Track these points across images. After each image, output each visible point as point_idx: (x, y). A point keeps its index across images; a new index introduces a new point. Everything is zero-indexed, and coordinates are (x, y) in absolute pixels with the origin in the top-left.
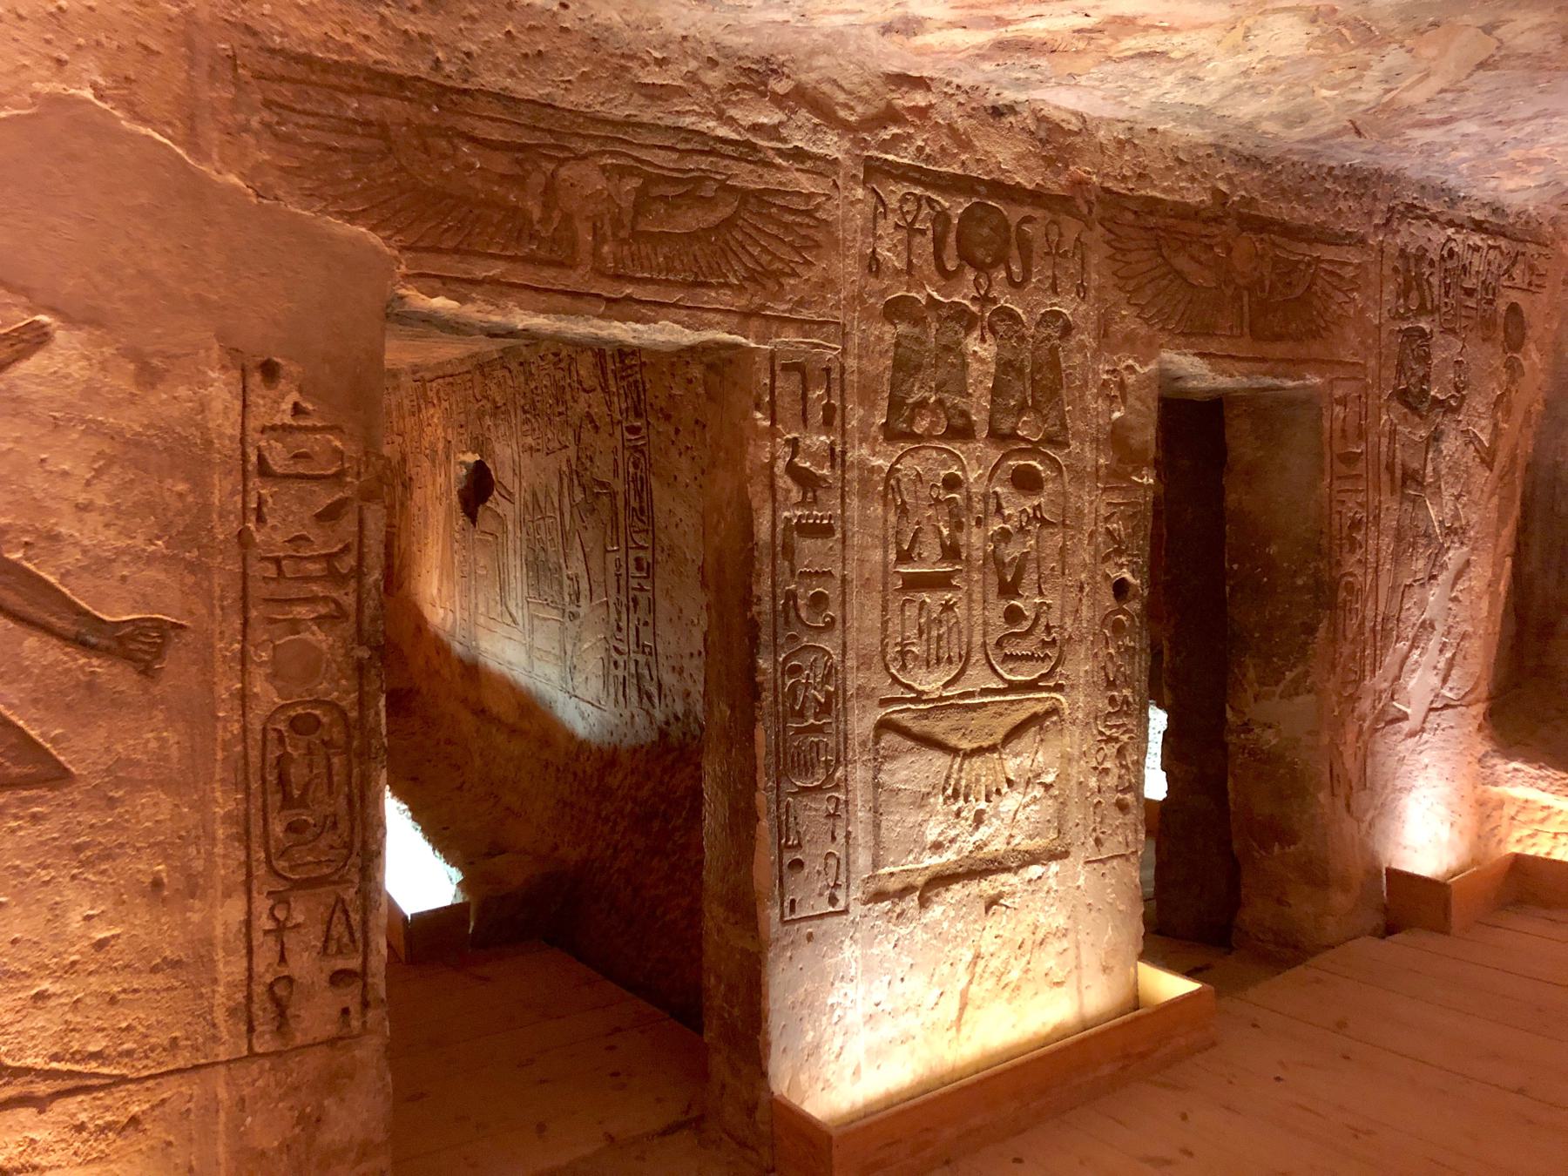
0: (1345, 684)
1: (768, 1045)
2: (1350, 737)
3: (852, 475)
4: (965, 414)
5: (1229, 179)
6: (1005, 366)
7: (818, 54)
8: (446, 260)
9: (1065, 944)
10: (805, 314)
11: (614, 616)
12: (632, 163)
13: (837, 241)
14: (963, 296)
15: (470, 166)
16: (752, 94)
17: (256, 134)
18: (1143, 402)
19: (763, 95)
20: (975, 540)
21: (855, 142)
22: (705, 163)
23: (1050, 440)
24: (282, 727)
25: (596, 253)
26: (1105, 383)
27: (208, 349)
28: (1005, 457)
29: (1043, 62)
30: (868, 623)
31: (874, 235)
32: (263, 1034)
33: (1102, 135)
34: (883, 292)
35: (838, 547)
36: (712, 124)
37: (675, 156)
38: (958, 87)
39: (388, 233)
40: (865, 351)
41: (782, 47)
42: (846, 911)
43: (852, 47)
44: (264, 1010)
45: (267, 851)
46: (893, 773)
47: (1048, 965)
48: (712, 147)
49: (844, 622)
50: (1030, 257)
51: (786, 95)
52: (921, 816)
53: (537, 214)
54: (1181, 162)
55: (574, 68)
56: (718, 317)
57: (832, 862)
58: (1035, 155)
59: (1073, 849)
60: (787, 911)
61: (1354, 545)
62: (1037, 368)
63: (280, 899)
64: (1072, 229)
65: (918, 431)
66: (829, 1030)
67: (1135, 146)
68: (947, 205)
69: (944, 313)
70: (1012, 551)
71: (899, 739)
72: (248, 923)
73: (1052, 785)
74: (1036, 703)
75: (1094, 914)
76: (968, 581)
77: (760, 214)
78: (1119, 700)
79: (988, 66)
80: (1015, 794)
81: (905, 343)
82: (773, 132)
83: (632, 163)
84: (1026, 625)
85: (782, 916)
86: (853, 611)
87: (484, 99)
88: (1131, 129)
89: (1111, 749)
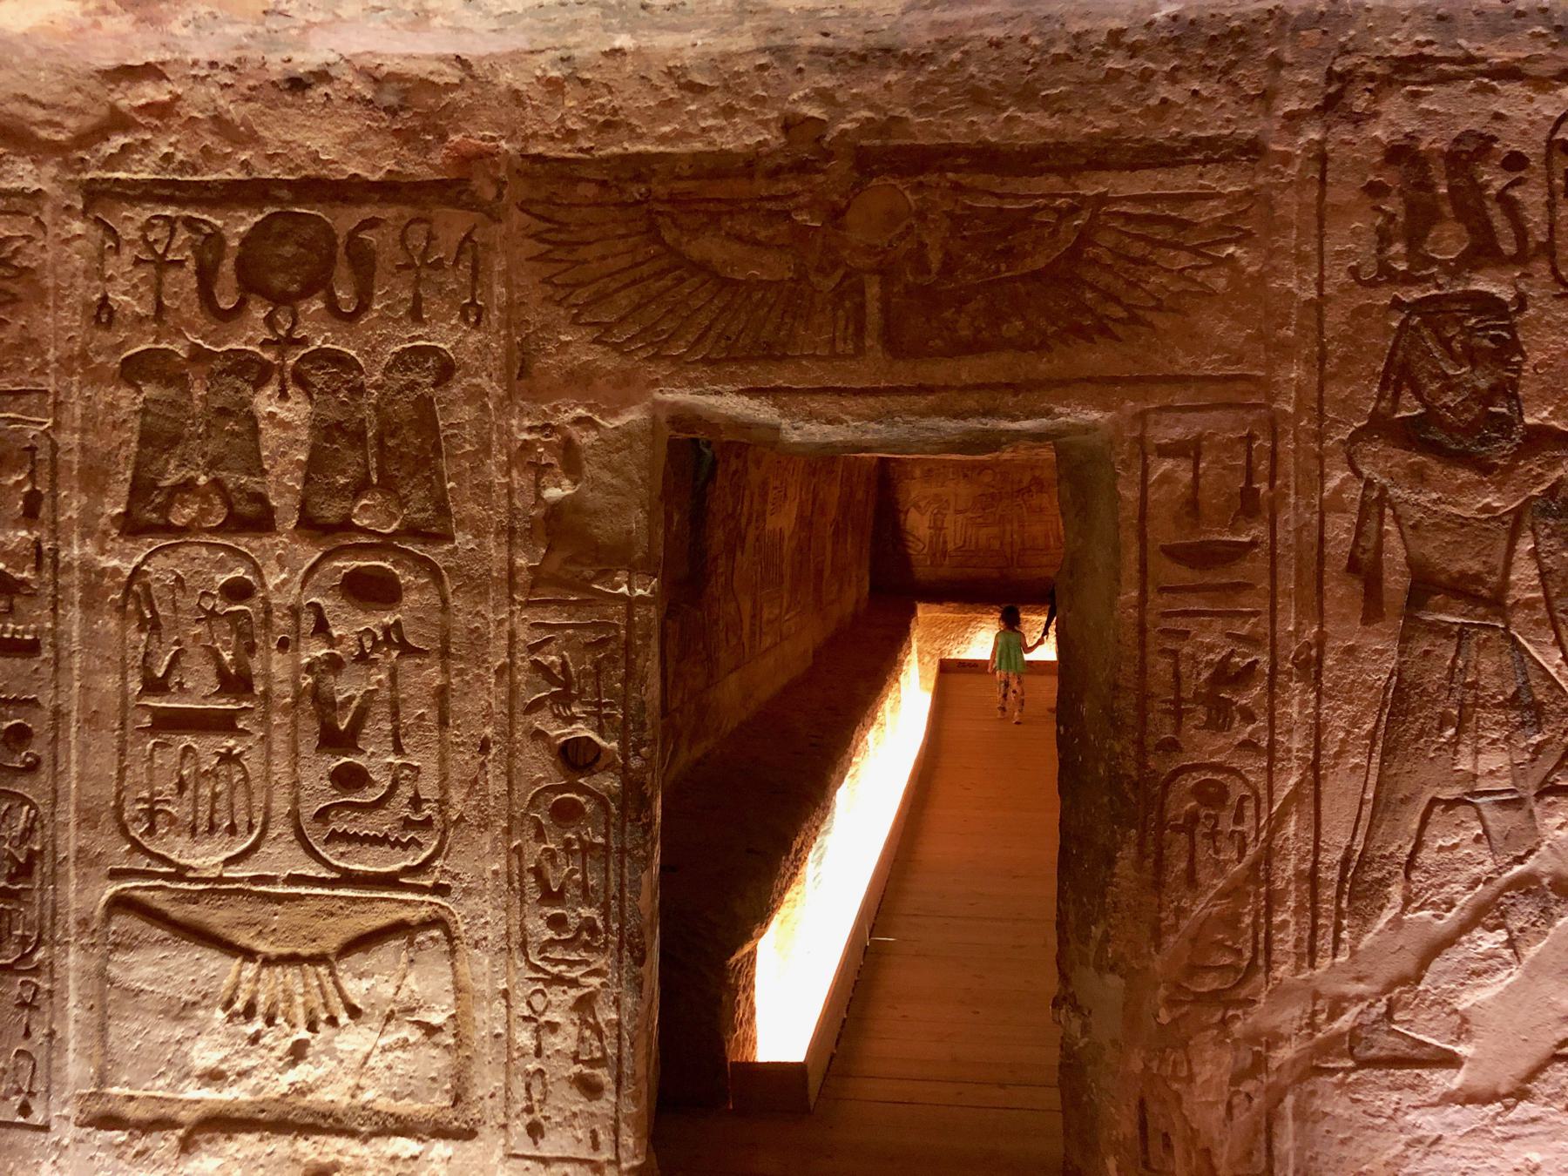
4: (261, 499)
5: (823, 96)
13: (43, 292)
14: (250, 336)
18: (616, 471)
20: (277, 670)
21: (67, 165)
23: (412, 531)
28: (327, 556)
30: (93, 769)
33: (507, 77)
34: (119, 348)
35: (48, 671)
38: (213, 64)
40: (89, 424)
42: (45, 1128)
46: (129, 968)
49: (55, 764)
50: (371, 275)
52: (179, 1032)
57: (22, 1062)
59: (484, 1131)
62: (388, 428)
65: (177, 521)
67: (585, 82)
68: (219, 223)
69: (217, 365)
74: (412, 906)
78: (573, 922)
80: (363, 1029)
81: (154, 409)
84: (371, 795)
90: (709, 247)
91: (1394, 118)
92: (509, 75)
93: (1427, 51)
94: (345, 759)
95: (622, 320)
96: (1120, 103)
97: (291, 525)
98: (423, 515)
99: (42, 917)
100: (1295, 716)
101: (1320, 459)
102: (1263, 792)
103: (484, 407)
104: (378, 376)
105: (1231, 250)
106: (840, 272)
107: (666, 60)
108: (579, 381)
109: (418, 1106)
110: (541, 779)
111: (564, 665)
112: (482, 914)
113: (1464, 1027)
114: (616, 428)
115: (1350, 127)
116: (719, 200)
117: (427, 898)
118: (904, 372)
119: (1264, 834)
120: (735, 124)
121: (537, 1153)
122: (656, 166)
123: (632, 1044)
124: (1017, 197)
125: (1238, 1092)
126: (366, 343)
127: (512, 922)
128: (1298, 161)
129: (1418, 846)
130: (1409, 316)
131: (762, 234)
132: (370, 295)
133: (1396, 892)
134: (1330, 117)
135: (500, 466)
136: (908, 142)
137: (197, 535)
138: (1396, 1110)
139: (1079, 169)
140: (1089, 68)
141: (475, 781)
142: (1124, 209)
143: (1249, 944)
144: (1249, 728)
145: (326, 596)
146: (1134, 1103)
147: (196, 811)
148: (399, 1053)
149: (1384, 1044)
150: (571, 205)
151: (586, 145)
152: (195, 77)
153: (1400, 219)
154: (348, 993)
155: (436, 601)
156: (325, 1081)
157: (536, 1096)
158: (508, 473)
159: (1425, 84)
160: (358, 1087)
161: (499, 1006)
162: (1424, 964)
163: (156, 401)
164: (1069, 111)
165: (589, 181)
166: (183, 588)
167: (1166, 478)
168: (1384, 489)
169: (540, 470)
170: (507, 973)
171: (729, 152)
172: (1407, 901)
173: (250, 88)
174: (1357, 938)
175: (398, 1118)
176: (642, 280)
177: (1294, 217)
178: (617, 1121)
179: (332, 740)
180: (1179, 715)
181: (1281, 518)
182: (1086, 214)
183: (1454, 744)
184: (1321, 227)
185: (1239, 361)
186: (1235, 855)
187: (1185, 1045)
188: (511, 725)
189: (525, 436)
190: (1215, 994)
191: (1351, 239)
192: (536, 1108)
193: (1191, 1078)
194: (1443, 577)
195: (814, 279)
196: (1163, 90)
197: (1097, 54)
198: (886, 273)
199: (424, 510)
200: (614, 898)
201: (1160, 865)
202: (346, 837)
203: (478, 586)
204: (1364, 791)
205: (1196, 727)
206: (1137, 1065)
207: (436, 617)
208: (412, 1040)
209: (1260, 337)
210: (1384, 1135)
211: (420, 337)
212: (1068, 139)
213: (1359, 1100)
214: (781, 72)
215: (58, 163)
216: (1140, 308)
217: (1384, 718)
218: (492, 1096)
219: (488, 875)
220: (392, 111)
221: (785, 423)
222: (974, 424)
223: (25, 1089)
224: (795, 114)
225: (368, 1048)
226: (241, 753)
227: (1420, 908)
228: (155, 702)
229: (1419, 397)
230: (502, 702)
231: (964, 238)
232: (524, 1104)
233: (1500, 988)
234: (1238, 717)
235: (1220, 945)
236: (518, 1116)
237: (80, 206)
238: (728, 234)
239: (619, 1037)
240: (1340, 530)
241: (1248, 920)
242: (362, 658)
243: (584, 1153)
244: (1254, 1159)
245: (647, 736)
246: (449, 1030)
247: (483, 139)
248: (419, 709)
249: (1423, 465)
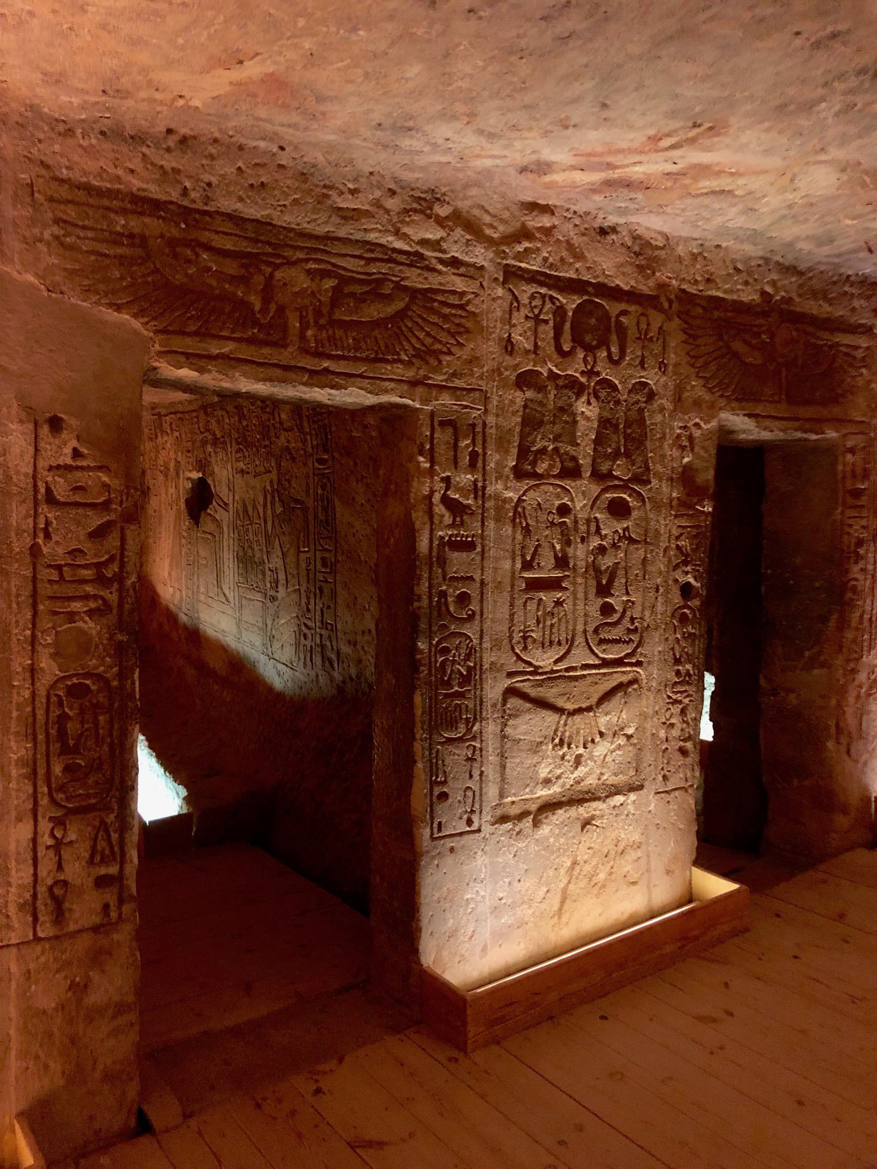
0: (848, 661)
1: (419, 930)
2: (851, 700)
3: (489, 504)
4: (574, 459)
5: (773, 283)
6: (605, 423)
7: (471, 186)
8: (188, 341)
9: (639, 853)
10: (458, 383)
11: (304, 600)
12: (330, 267)
14: (575, 369)
15: (209, 269)
16: (422, 216)
17: (48, 244)
18: (706, 451)
19: (429, 217)
20: (579, 553)
21: (497, 253)
22: (384, 268)
23: (638, 479)
24: (61, 693)
25: (302, 337)
26: (679, 436)
27: (10, 407)
29: (640, 196)
31: (510, 323)
32: (44, 922)
33: (680, 250)
35: (478, 558)
36: (390, 239)
37: (362, 263)
38: (575, 212)
39: (146, 319)
40: (501, 410)
41: (444, 181)
42: (479, 831)
43: (496, 182)
44: (46, 905)
45: (49, 787)
46: (515, 727)
47: (627, 869)
48: (390, 256)
51: (447, 217)
53: (257, 307)
54: (736, 269)
55: (287, 195)
56: (392, 385)
57: (470, 794)
58: (631, 264)
59: (646, 784)
60: (435, 830)
61: (858, 558)
62: (628, 425)
63: (59, 822)
64: (656, 320)
66: (465, 918)
67: (705, 258)
68: (564, 301)
69: (561, 382)
70: (606, 562)
71: (521, 702)
72: (34, 841)
75: (661, 831)
76: (574, 584)
77: (424, 307)
78: (683, 672)
79: (598, 198)
82: (436, 245)
83: (330, 267)
84: (616, 617)
85: (432, 834)
86: (489, 606)
87: (220, 218)
88: (702, 245)
89: (676, 709)
97: (588, 474)
99: (475, 705)
137: (547, 479)
147: (544, 635)
148: (617, 752)
151: (701, 288)
152: (565, 217)
156: (588, 774)
160: (602, 774)
163: (532, 401)
166: (541, 509)
173: (586, 229)
199: (641, 467)
207: (643, 524)
208: (622, 744)
211: (643, 377)
215: (494, 251)
219: (656, 653)
220: (637, 254)
223: (469, 810)
226: (564, 600)
228: (526, 575)
237: (501, 280)
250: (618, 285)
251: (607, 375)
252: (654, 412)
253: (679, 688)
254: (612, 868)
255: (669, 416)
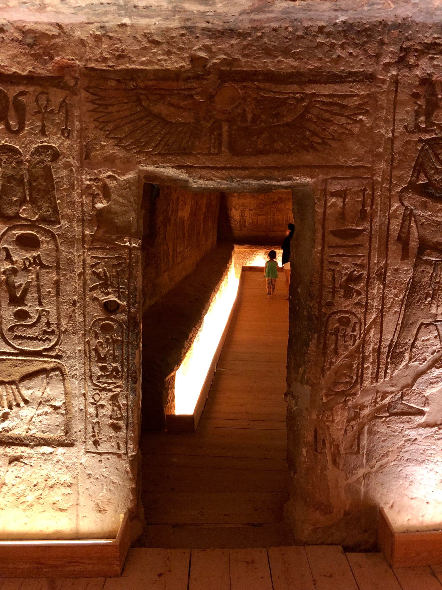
5: (206, 48)
9: (68, 490)
23: (43, 220)
26: (89, 187)
28: (9, 229)
33: (78, 34)
50: (24, 115)
58: (25, 54)
59: (77, 444)
62: (33, 178)
67: (110, 37)
73: (59, 408)
75: (92, 480)
78: (110, 368)
80: (30, 408)
90: (161, 109)
91: (424, 67)
92: (79, 33)
93: (437, 41)
94: (19, 308)
95: (126, 136)
96: (322, 56)
98: (48, 213)
100: (376, 293)
101: (390, 198)
102: (363, 321)
103: (71, 171)
104: (28, 157)
105: (361, 117)
106: (213, 120)
107: (144, 30)
108: (109, 161)
109: (52, 435)
110: (96, 316)
111: (105, 272)
112: (75, 366)
113: (426, 402)
114: (124, 180)
115: (407, 70)
116: (165, 90)
117: (53, 360)
118: (237, 161)
119: (362, 336)
120: (171, 59)
121: (97, 451)
122: (140, 74)
123: (132, 412)
124: (281, 93)
125: (348, 425)
126: (23, 143)
127: (86, 368)
128: (388, 83)
129: (416, 339)
130: (425, 145)
131: (182, 104)
132: (24, 123)
133: (407, 356)
134: (400, 66)
135: (78, 195)
136: (240, 69)
138: (402, 430)
139: (305, 83)
140: (311, 41)
141: (71, 316)
142: (321, 99)
143: (355, 374)
144: (359, 298)
145: (10, 245)
146: (313, 429)
148: (44, 416)
149: (399, 408)
150: (105, 89)
151: (111, 64)
153: (424, 107)
154: (24, 395)
155: (54, 247)
157: (96, 431)
158: (81, 197)
159: (436, 54)
160: (29, 429)
161: (82, 399)
162: (415, 380)
164: (303, 59)
165: (112, 79)
167: (333, 205)
168: (412, 211)
169: (94, 196)
170: (85, 387)
171: (169, 70)
172: (410, 359)
174: (393, 372)
175: (44, 439)
176: (134, 121)
177: (385, 105)
178: (127, 439)
179: (14, 301)
180: (334, 293)
181: (374, 220)
182: (307, 101)
183: (430, 304)
184: (395, 109)
185: (361, 161)
186: (352, 343)
187: (331, 409)
188: (84, 295)
189: (88, 182)
190: (343, 391)
191: (405, 114)
192: (97, 435)
193: (333, 421)
194: (430, 243)
195: (201, 122)
196: (339, 52)
197: (314, 36)
198: (231, 121)
199: (49, 211)
200: (125, 359)
201: (325, 347)
202: (21, 337)
203: (70, 242)
204: (398, 320)
205: (340, 297)
206: (314, 417)
207: (54, 254)
208: (49, 411)
209: (370, 151)
210: (398, 438)
212: (302, 70)
213: (389, 427)
214: (190, 37)
216: (327, 139)
217: (407, 294)
218: (80, 431)
219: (77, 351)
221: (191, 180)
222: (263, 182)
224: (195, 55)
225: (32, 415)
227: (415, 361)
229: (426, 176)
230: (81, 287)
231: (260, 108)
232: (92, 434)
233: (439, 388)
234: (355, 294)
235: (345, 375)
236: (89, 438)
238: (168, 103)
239: (127, 410)
240: (395, 225)
241: (355, 366)
242: (25, 269)
243: (114, 451)
244: (353, 447)
245: (137, 300)
246: (63, 408)
247: (69, 59)
248: (48, 289)
249: (426, 202)
250: (16, 72)
251: (6, 142)
252: (59, 168)
253: (104, 380)
254: (41, 495)
255: (76, 171)
